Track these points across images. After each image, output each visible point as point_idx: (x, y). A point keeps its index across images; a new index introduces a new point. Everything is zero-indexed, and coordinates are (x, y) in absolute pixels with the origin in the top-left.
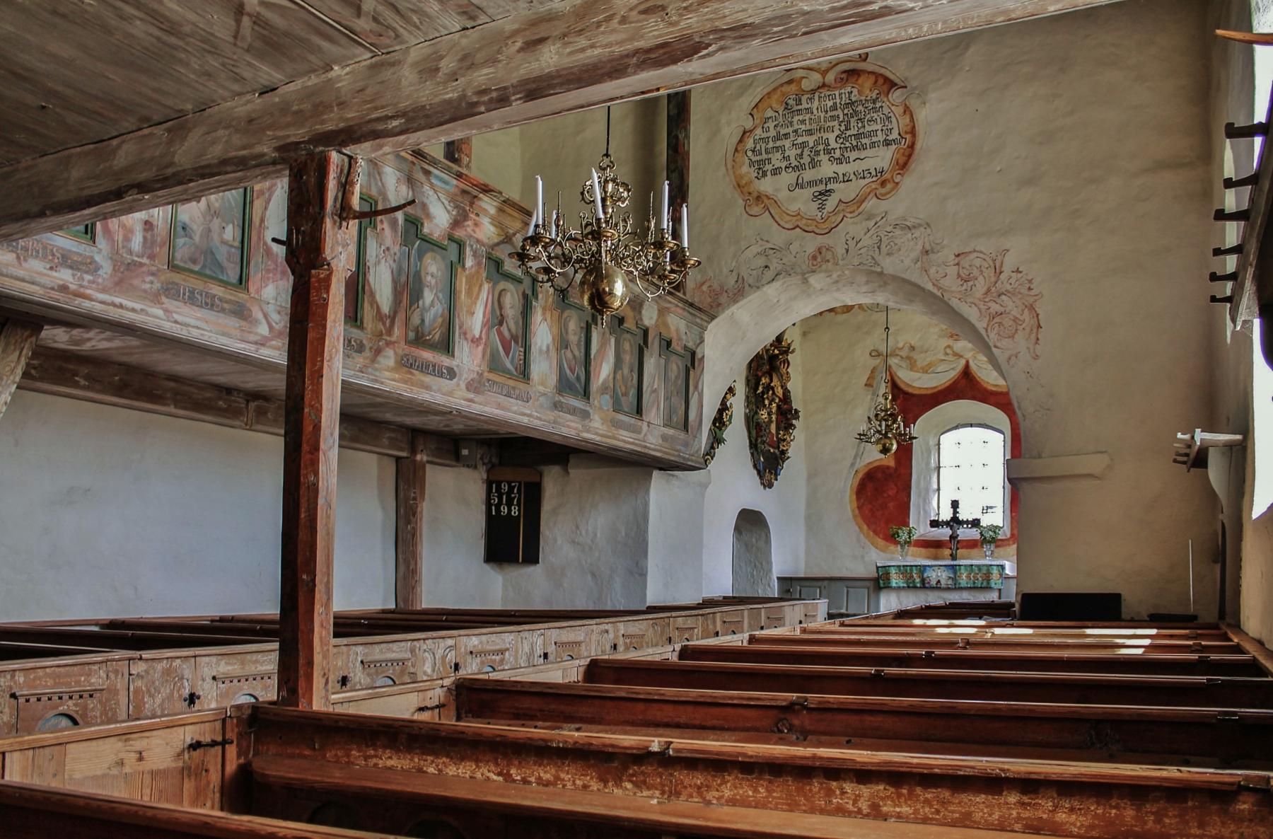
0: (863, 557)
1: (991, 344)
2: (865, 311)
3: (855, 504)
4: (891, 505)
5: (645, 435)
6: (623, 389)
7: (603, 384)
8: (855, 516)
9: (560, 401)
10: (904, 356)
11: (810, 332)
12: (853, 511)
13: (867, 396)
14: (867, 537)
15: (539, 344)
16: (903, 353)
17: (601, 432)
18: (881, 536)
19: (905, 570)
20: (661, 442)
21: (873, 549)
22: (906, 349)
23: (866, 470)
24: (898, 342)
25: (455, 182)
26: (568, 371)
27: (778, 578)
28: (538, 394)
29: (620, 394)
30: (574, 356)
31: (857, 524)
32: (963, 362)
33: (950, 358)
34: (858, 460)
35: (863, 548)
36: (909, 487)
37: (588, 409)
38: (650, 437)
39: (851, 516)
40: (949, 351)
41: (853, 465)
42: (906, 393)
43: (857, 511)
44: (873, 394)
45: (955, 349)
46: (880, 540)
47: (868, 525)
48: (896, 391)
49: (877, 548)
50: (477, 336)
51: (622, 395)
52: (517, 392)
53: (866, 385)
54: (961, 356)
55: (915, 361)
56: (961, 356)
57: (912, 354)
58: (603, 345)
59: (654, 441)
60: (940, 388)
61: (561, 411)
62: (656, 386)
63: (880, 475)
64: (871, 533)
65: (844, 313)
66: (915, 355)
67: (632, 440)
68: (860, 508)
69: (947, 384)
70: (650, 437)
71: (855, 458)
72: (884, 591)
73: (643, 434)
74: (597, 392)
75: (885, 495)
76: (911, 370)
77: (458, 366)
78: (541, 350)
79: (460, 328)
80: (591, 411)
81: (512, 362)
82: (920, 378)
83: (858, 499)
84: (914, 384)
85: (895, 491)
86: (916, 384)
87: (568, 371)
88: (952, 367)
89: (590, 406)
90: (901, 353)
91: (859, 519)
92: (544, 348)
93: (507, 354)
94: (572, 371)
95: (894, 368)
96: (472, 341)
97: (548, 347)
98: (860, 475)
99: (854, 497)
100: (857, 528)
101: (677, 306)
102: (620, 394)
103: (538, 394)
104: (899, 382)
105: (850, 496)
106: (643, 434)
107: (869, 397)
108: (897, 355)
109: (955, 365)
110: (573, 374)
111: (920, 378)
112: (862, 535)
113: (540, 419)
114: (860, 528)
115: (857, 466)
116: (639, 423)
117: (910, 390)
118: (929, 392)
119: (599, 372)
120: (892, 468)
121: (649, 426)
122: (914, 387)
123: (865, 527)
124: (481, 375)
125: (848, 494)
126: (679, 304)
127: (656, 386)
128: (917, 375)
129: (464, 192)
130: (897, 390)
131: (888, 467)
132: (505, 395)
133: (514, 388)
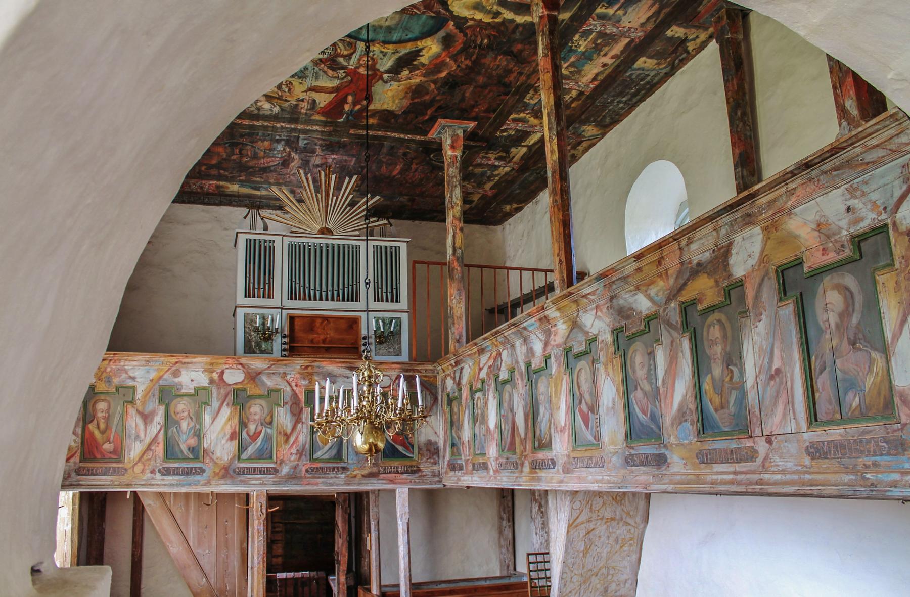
5: (765, 459)
6: (717, 400)
7: (680, 409)
9: (631, 455)
15: (605, 403)
17: (678, 477)
20: (807, 461)
25: (533, 320)
26: (640, 415)
28: (610, 455)
29: (712, 410)
30: (645, 394)
37: (663, 451)
38: (777, 459)
50: (563, 425)
51: (716, 410)
52: (594, 460)
58: (673, 361)
59: (790, 465)
61: (634, 465)
62: (777, 364)
67: (731, 476)
70: (777, 459)
73: (760, 460)
74: (672, 424)
77: (555, 456)
78: (608, 408)
79: (554, 424)
80: (667, 453)
81: (591, 434)
87: (640, 415)
89: (665, 446)
92: (610, 405)
93: (587, 427)
94: (644, 413)
96: (561, 431)
97: (614, 401)
101: (792, 192)
102: (712, 410)
103: (610, 455)
106: (760, 460)
110: (646, 415)
113: (601, 481)
116: (749, 443)
119: (672, 396)
121: (769, 442)
124: (568, 456)
126: (792, 186)
127: (777, 364)
129: (540, 320)
132: (586, 467)
133: (591, 458)
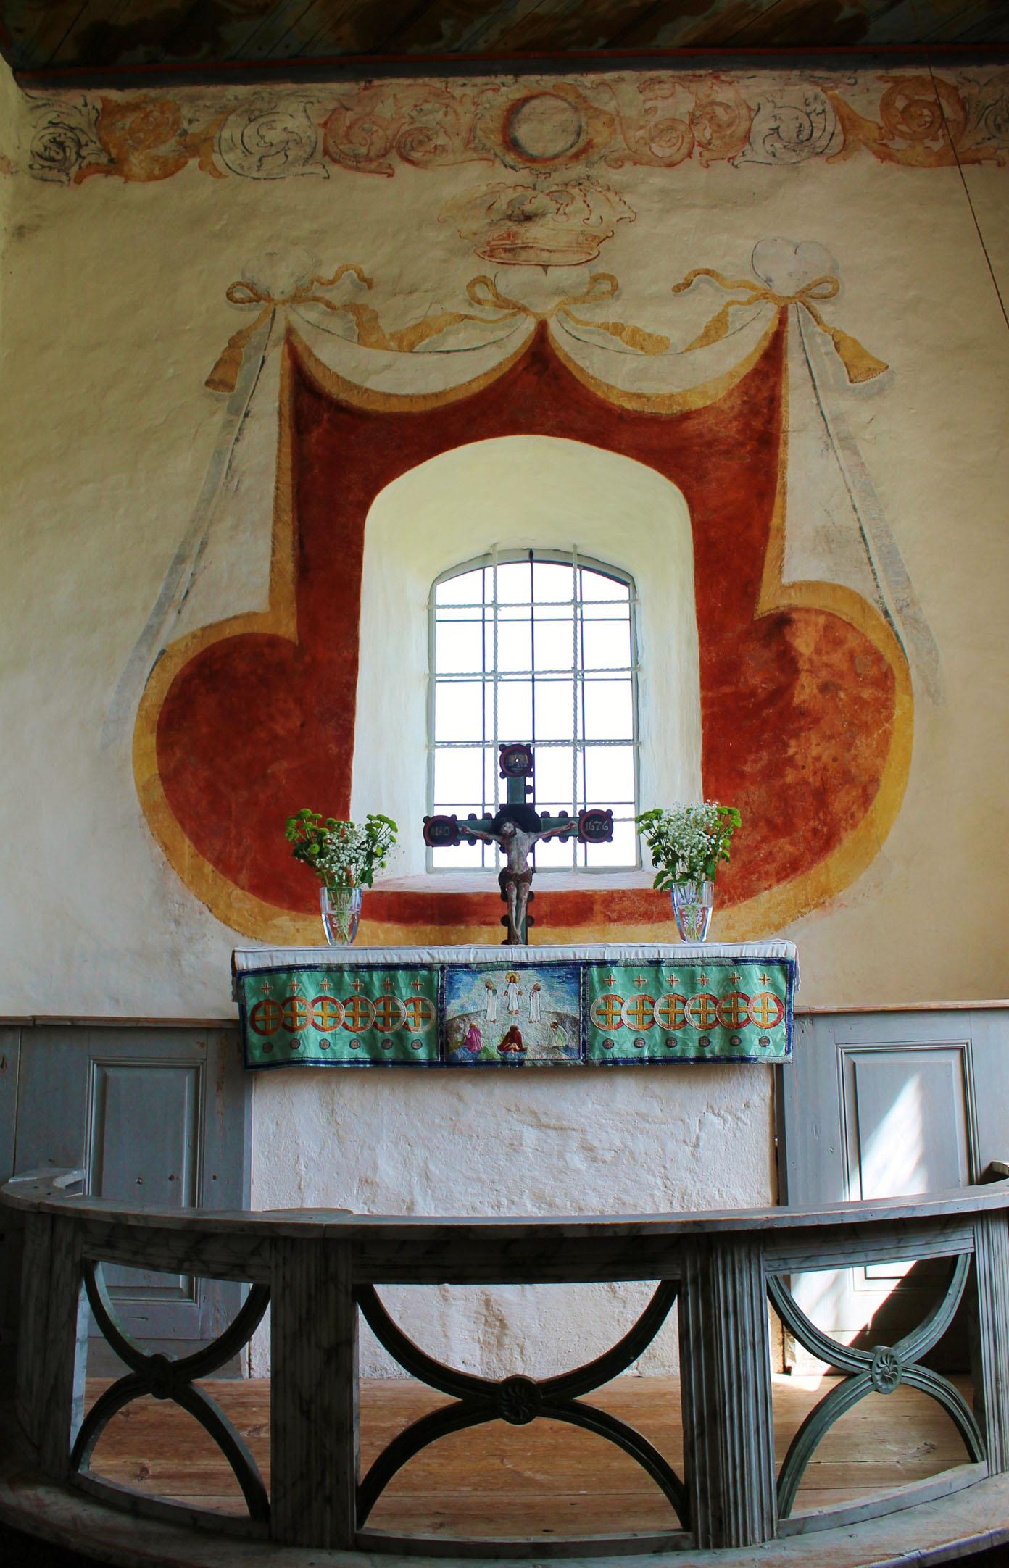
0: (175, 955)
2: (220, 176)
3: (152, 769)
8: (149, 809)
10: (337, 303)
11: (37, 228)
12: (144, 789)
13: (213, 414)
14: (194, 880)
16: (337, 296)
18: (244, 877)
21: (214, 925)
22: (346, 284)
24: (318, 264)
31: (158, 833)
32: (527, 327)
33: (489, 312)
34: (172, 616)
35: (177, 922)
36: (347, 707)
39: (138, 807)
40: (481, 292)
41: (151, 632)
42: (341, 409)
43: (158, 791)
44: (233, 410)
45: (501, 288)
46: (238, 892)
47: (197, 841)
49: (226, 921)
54: (523, 309)
55: (376, 317)
56: (523, 309)
57: (365, 298)
60: (452, 398)
64: (208, 868)
65: (151, 178)
66: (373, 301)
68: (170, 778)
69: (477, 388)
71: (161, 609)
76: (362, 341)
82: (388, 367)
83: (164, 747)
84: (369, 384)
85: (296, 722)
88: (492, 338)
90: (328, 296)
91: (166, 818)
95: (305, 335)
98: (175, 667)
99: (151, 741)
100: (158, 849)
105: (137, 738)
107: (219, 418)
108: (316, 299)
109: (500, 334)
111: (388, 367)
112: (174, 875)
114: (166, 847)
117: (356, 401)
120: (289, 642)
122: (367, 390)
123: (186, 846)
125: (130, 728)
128: (382, 357)
131: (273, 642)
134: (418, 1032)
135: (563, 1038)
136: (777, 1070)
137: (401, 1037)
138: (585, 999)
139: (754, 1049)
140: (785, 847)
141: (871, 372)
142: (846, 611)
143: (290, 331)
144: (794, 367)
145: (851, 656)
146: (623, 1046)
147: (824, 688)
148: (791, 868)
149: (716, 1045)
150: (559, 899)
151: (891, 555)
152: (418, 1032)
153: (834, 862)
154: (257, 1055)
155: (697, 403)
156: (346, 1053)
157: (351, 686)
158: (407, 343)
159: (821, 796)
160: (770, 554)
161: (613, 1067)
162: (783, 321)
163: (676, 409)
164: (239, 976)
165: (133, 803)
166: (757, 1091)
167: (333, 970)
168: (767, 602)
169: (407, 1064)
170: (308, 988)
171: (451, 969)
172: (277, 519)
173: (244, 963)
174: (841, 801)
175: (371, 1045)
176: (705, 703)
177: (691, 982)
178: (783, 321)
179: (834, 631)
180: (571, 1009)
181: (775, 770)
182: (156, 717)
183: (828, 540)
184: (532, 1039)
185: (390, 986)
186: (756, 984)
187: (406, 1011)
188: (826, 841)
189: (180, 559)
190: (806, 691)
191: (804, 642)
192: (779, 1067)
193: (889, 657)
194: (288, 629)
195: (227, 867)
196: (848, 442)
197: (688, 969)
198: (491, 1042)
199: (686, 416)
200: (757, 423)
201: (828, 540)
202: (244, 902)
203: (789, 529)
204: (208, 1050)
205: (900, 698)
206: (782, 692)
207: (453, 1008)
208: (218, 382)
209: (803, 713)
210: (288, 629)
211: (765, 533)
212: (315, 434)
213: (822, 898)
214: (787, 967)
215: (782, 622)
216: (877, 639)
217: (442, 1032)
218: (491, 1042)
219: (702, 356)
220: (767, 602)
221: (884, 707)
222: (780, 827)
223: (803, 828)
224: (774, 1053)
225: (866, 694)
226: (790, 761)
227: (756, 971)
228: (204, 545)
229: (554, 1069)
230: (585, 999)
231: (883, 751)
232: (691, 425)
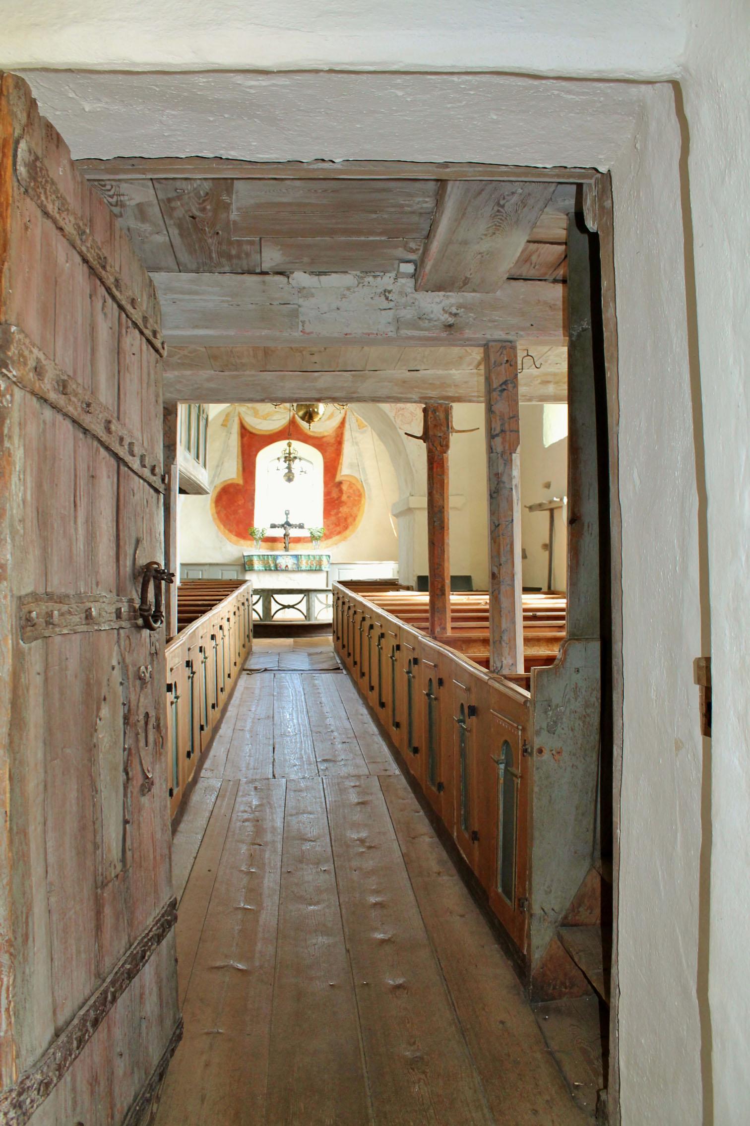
0: (220, 548)
1: (397, 427)
3: (214, 510)
4: (240, 511)
8: (214, 519)
12: (213, 515)
18: (234, 533)
19: (263, 558)
23: (222, 486)
27: (182, 565)
42: (251, 433)
43: (216, 516)
47: (224, 526)
48: (243, 430)
49: (230, 541)
53: (222, 425)
63: (232, 490)
64: (227, 531)
68: (218, 513)
69: (280, 429)
71: (214, 477)
72: (248, 572)
75: (236, 504)
76: (255, 417)
83: (217, 506)
85: (243, 501)
86: (259, 427)
95: (243, 415)
98: (218, 489)
99: (213, 505)
104: (248, 427)
107: (224, 434)
115: (214, 484)
118: (268, 433)
123: (222, 527)
128: (260, 421)
130: (244, 431)
131: (238, 485)
134: (272, 565)
135: (295, 566)
136: (327, 572)
137: (270, 566)
138: (298, 560)
139: (323, 569)
140: (338, 529)
141: (363, 427)
142: (354, 481)
143: (239, 413)
144: (347, 425)
145: (354, 491)
146: (304, 568)
147: (348, 497)
148: (339, 533)
149: (318, 568)
150: (295, 538)
151: (364, 469)
152: (272, 565)
153: (347, 532)
154: (247, 569)
155: (326, 434)
156: (261, 568)
157: (254, 495)
158: (265, 418)
159: (346, 519)
160: (339, 468)
161: (302, 571)
162: (346, 414)
163: (322, 435)
164: (244, 556)
165: (211, 518)
166: (325, 574)
167: (259, 556)
168: (338, 479)
169: (271, 570)
170: (255, 559)
171: (277, 556)
172: (238, 458)
173: (245, 554)
174: (350, 520)
175: (265, 567)
176: (325, 500)
177: (314, 558)
178: (346, 414)
179: (351, 485)
180: (296, 562)
181: (337, 514)
182: (214, 500)
183: (351, 466)
184: (290, 567)
185: (268, 558)
186: (324, 559)
187: (270, 562)
188: (346, 528)
189: (218, 466)
190: (344, 498)
191: (345, 487)
192: (327, 572)
193: (362, 491)
194: (241, 482)
195: (230, 531)
196: (357, 444)
197: (314, 557)
198: (283, 567)
199: (323, 437)
200: (338, 439)
201: (351, 466)
202: (234, 538)
203: (344, 463)
204: (239, 568)
205: (363, 499)
206: (339, 498)
207: (278, 562)
208: (224, 425)
209: (343, 502)
210: (241, 482)
211: (338, 463)
212: (245, 439)
213: (345, 538)
214: (329, 556)
215: (340, 483)
216: (359, 487)
217: (276, 566)
218: (283, 567)
219: (328, 422)
220: (338, 479)
221: (359, 501)
222: (337, 525)
223: (342, 525)
224: (326, 570)
225: (357, 498)
226: (340, 512)
227: (324, 557)
228: (223, 463)
229: (293, 571)
230: (298, 560)
231: (359, 510)
232: (324, 440)
